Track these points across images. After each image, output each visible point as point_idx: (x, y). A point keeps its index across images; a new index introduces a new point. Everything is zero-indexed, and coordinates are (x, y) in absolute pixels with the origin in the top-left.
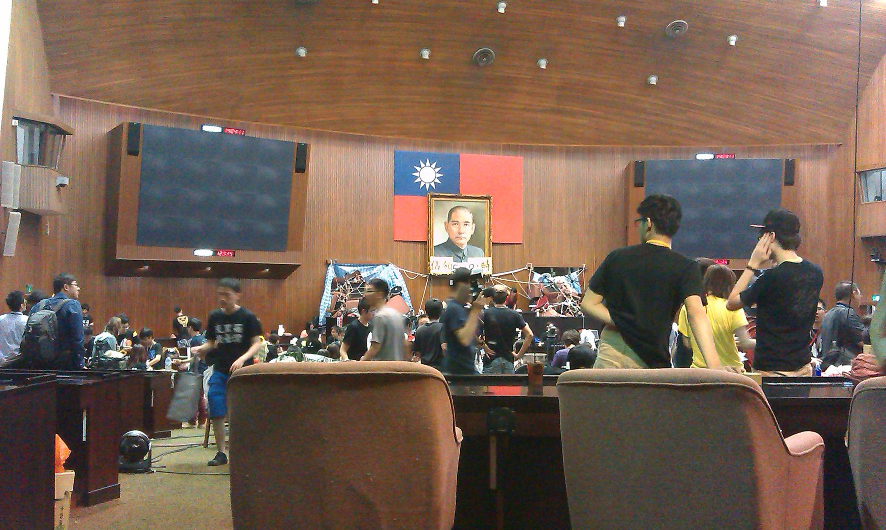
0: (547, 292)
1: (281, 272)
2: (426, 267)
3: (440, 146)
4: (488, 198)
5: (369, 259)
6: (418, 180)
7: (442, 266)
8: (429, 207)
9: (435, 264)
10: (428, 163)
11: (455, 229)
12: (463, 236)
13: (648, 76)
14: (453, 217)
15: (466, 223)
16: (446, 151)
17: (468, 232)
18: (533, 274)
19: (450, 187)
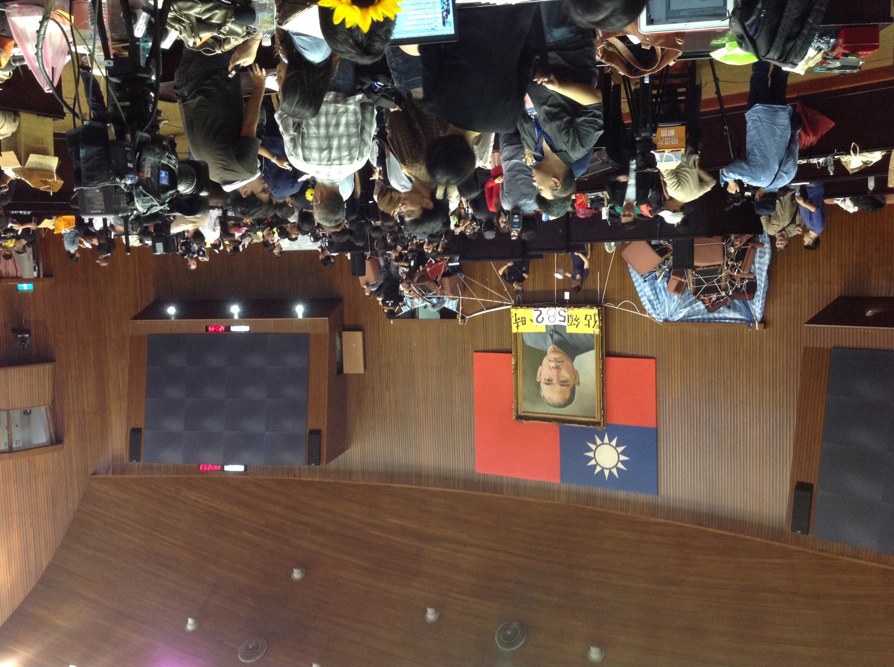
0: (431, 285)
1: (844, 310)
2: (606, 318)
3: (590, 498)
4: (519, 417)
5: (695, 330)
6: (620, 449)
7: (582, 320)
8: (604, 409)
9: (592, 323)
10: (607, 473)
11: (565, 375)
12: (553, 364)
13: (303, 579)
14: (567, 390)
15: (549, 382)
16: (583, 488)
17: (546, 370)
18: (458, 308)
19: (576, 434)
